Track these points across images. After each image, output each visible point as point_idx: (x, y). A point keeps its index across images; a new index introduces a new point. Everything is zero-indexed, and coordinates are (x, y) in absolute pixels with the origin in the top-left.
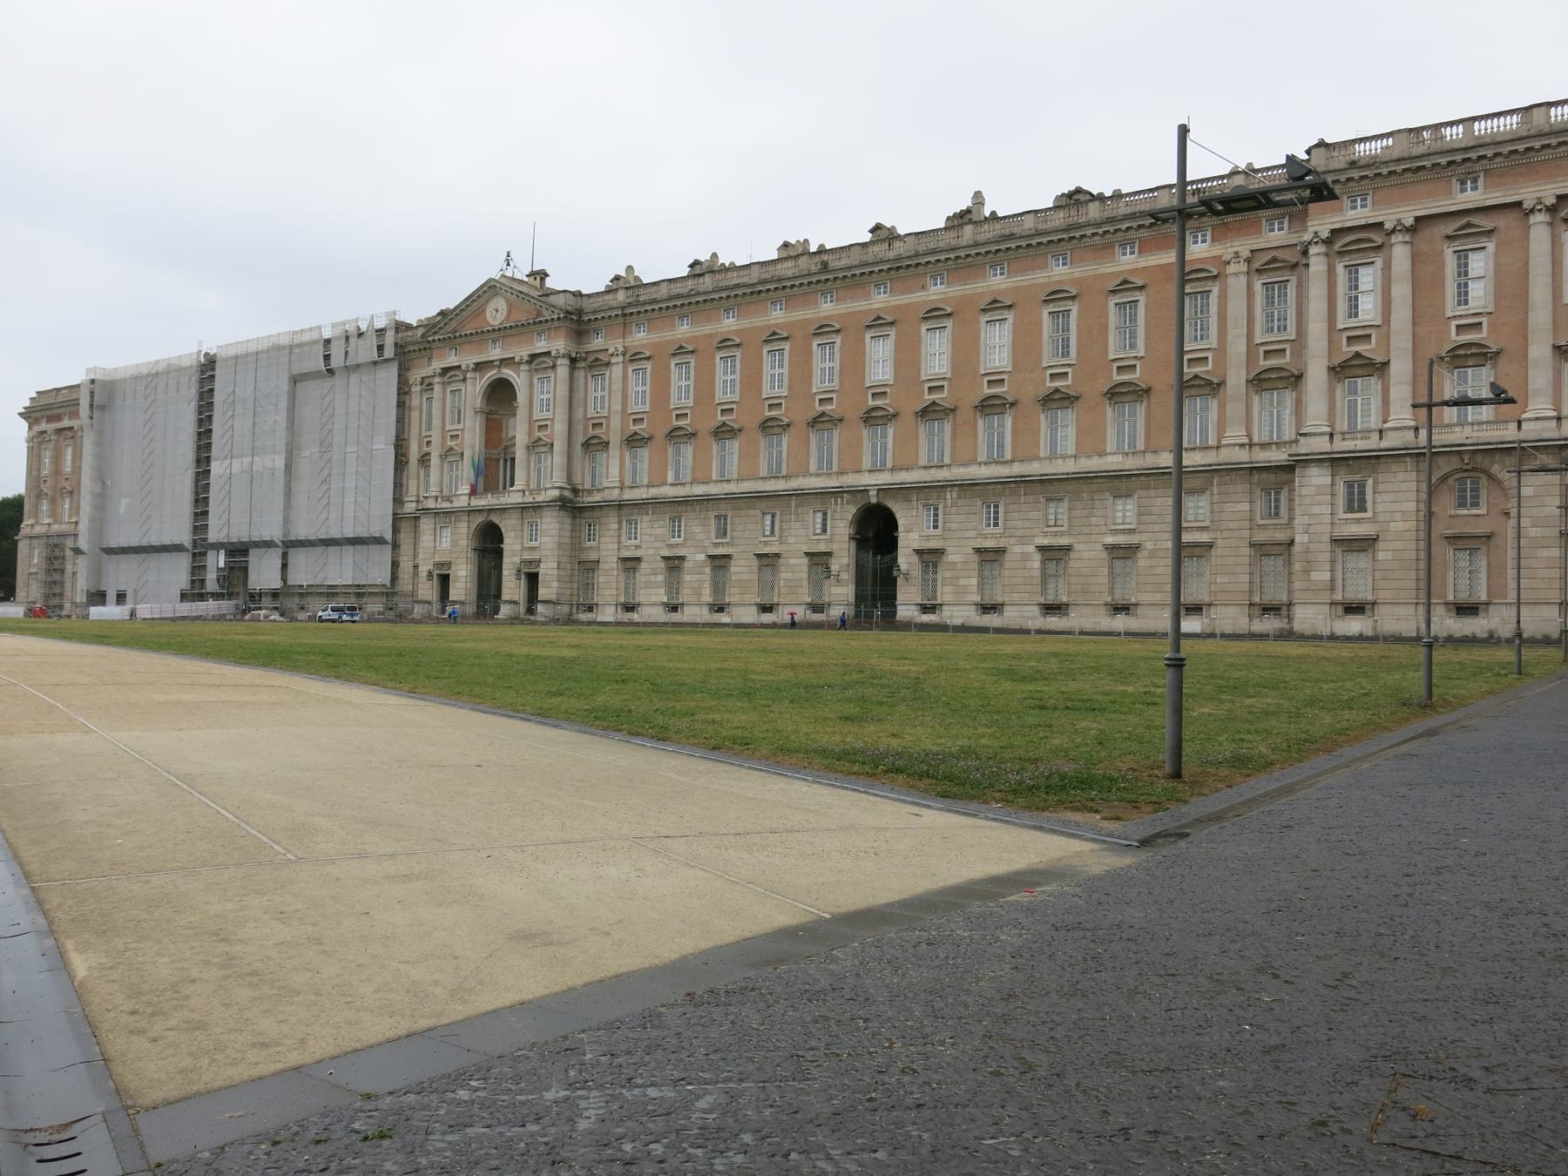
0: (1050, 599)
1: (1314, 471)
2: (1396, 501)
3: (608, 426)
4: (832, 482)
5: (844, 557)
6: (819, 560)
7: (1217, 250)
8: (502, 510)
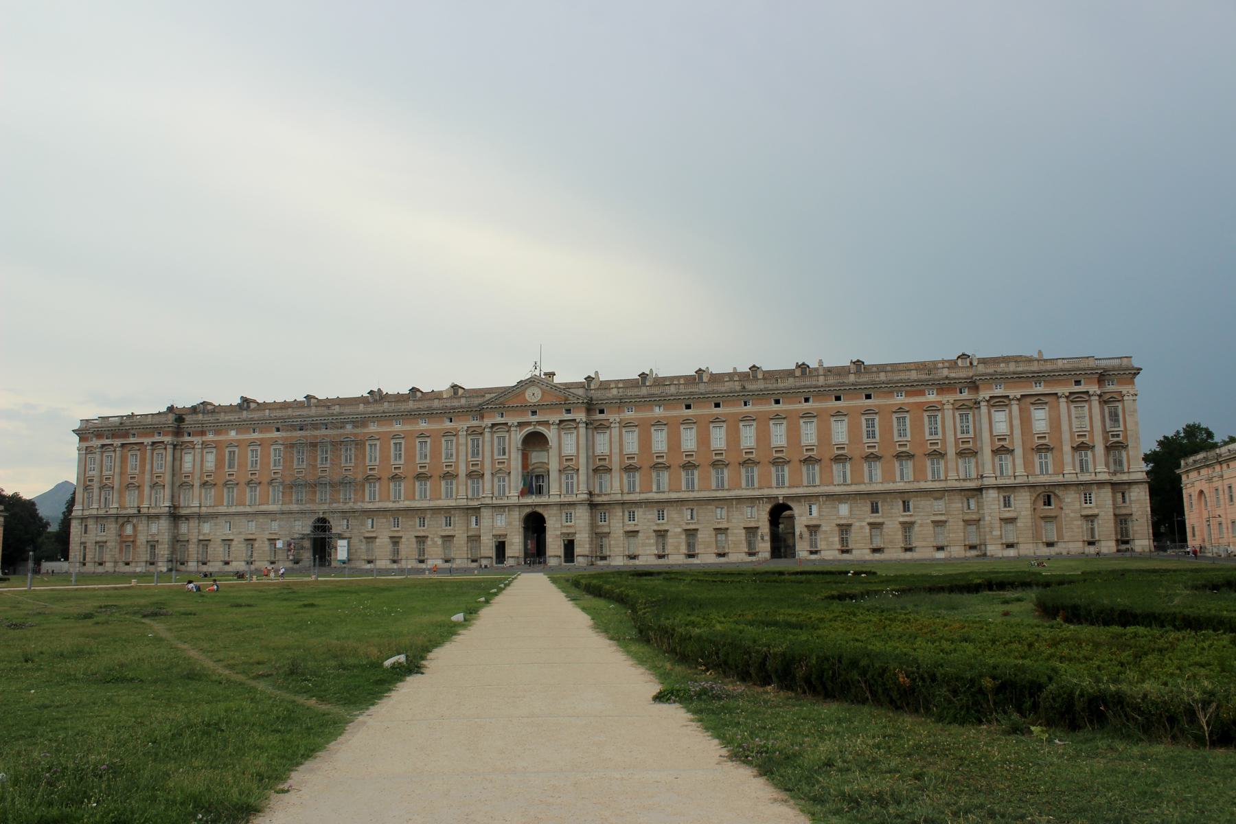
0: (874, 546)
1: (991, 491)
2: (1023, 504)
3: (611, 460)
4: (756, 493)
5: (765, 529)
6: (751, 531)
7: (939, 398)
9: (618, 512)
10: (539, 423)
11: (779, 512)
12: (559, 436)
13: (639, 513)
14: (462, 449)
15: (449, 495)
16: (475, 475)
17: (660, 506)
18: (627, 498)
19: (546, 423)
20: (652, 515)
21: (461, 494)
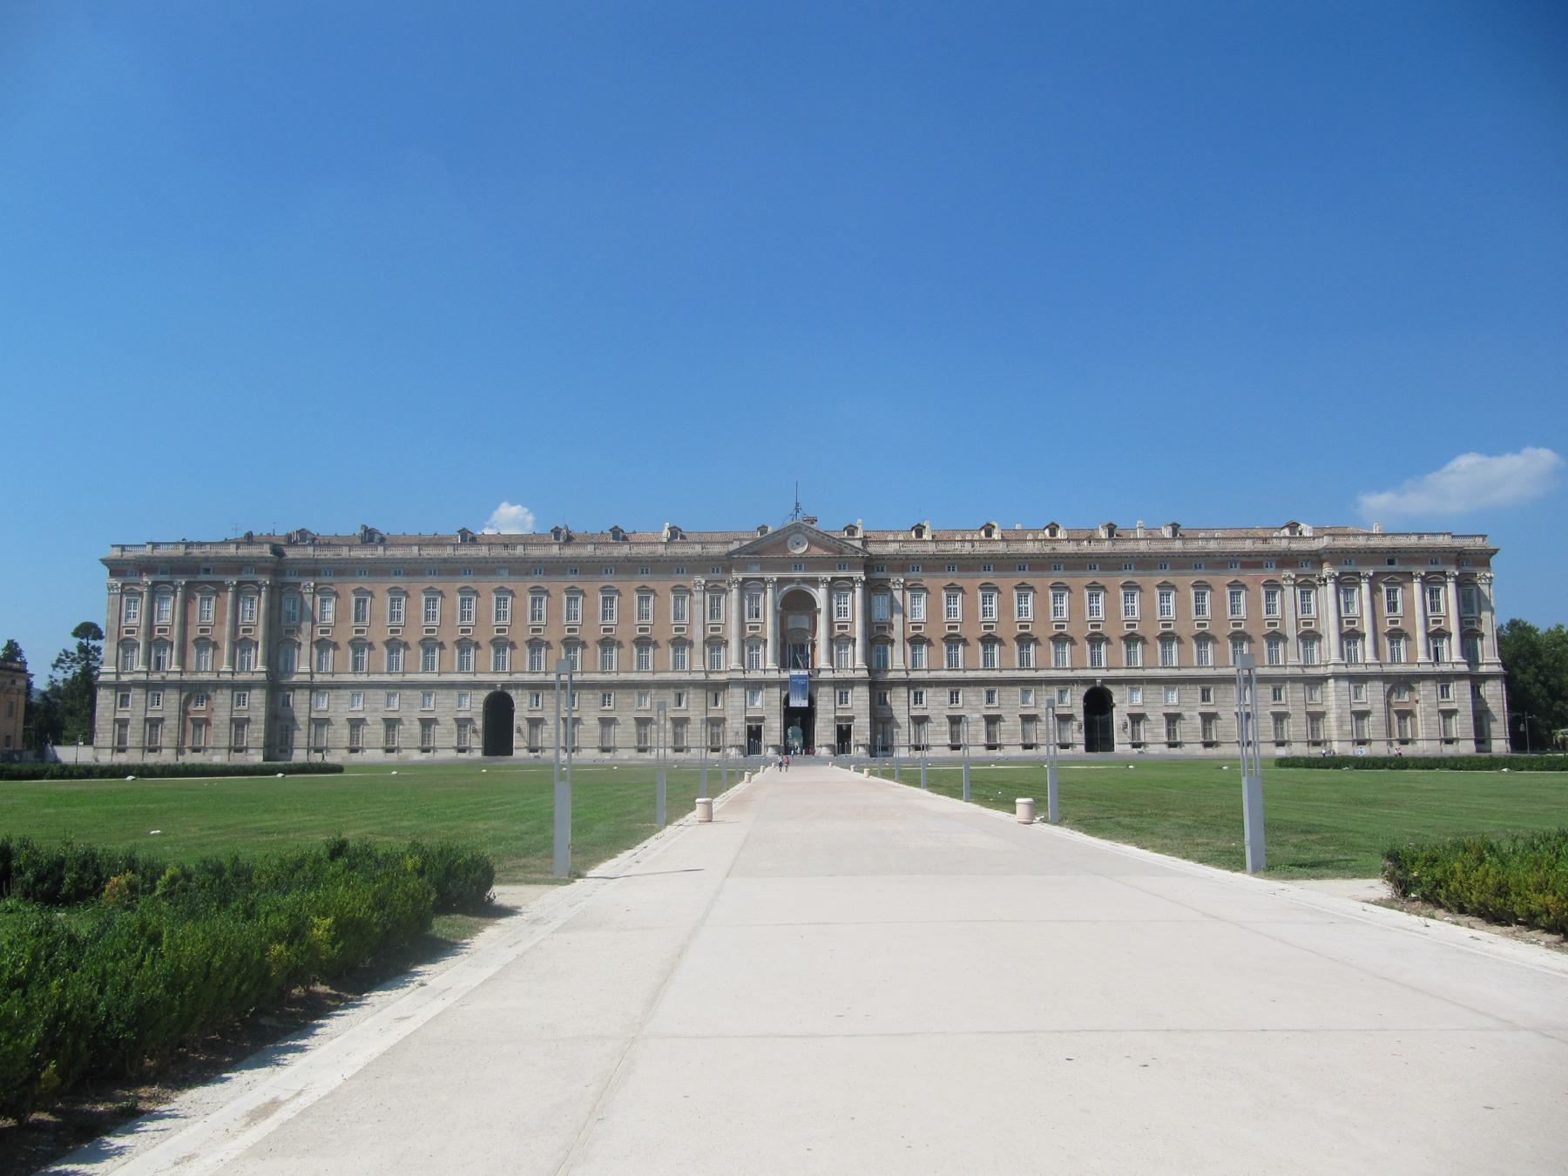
9: (902, 692)
11: (1098, 702)
13: (928, 694)
14: (698, 608)
16: (715, 643)
17: (954, 686)
18: (913, 675)
19: (815, 582)
20: (944, 695)
21: (696, 665)
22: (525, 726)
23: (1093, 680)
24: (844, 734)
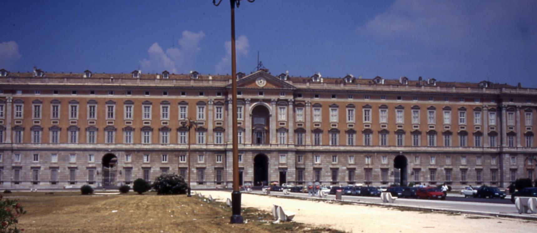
3: (305, 125)
8: (270, 151)
10: (265, 100)
12: (277, 109)
15: (478, 145)
19: (269, 101)
22: (124, 171)
23: (398, 152)
24: (283, 178)
